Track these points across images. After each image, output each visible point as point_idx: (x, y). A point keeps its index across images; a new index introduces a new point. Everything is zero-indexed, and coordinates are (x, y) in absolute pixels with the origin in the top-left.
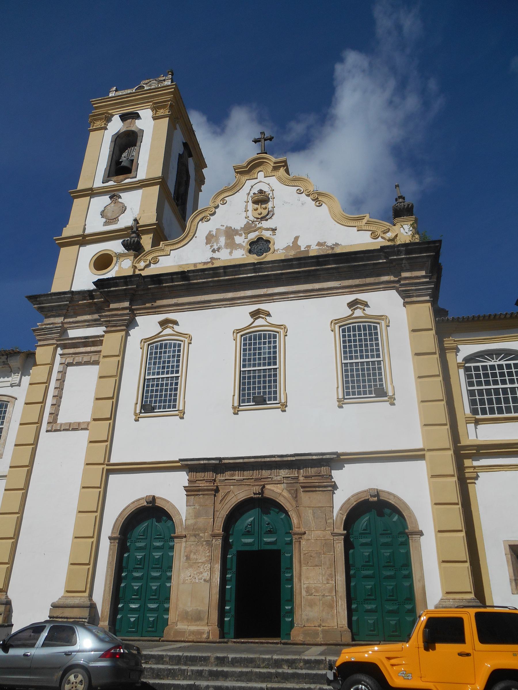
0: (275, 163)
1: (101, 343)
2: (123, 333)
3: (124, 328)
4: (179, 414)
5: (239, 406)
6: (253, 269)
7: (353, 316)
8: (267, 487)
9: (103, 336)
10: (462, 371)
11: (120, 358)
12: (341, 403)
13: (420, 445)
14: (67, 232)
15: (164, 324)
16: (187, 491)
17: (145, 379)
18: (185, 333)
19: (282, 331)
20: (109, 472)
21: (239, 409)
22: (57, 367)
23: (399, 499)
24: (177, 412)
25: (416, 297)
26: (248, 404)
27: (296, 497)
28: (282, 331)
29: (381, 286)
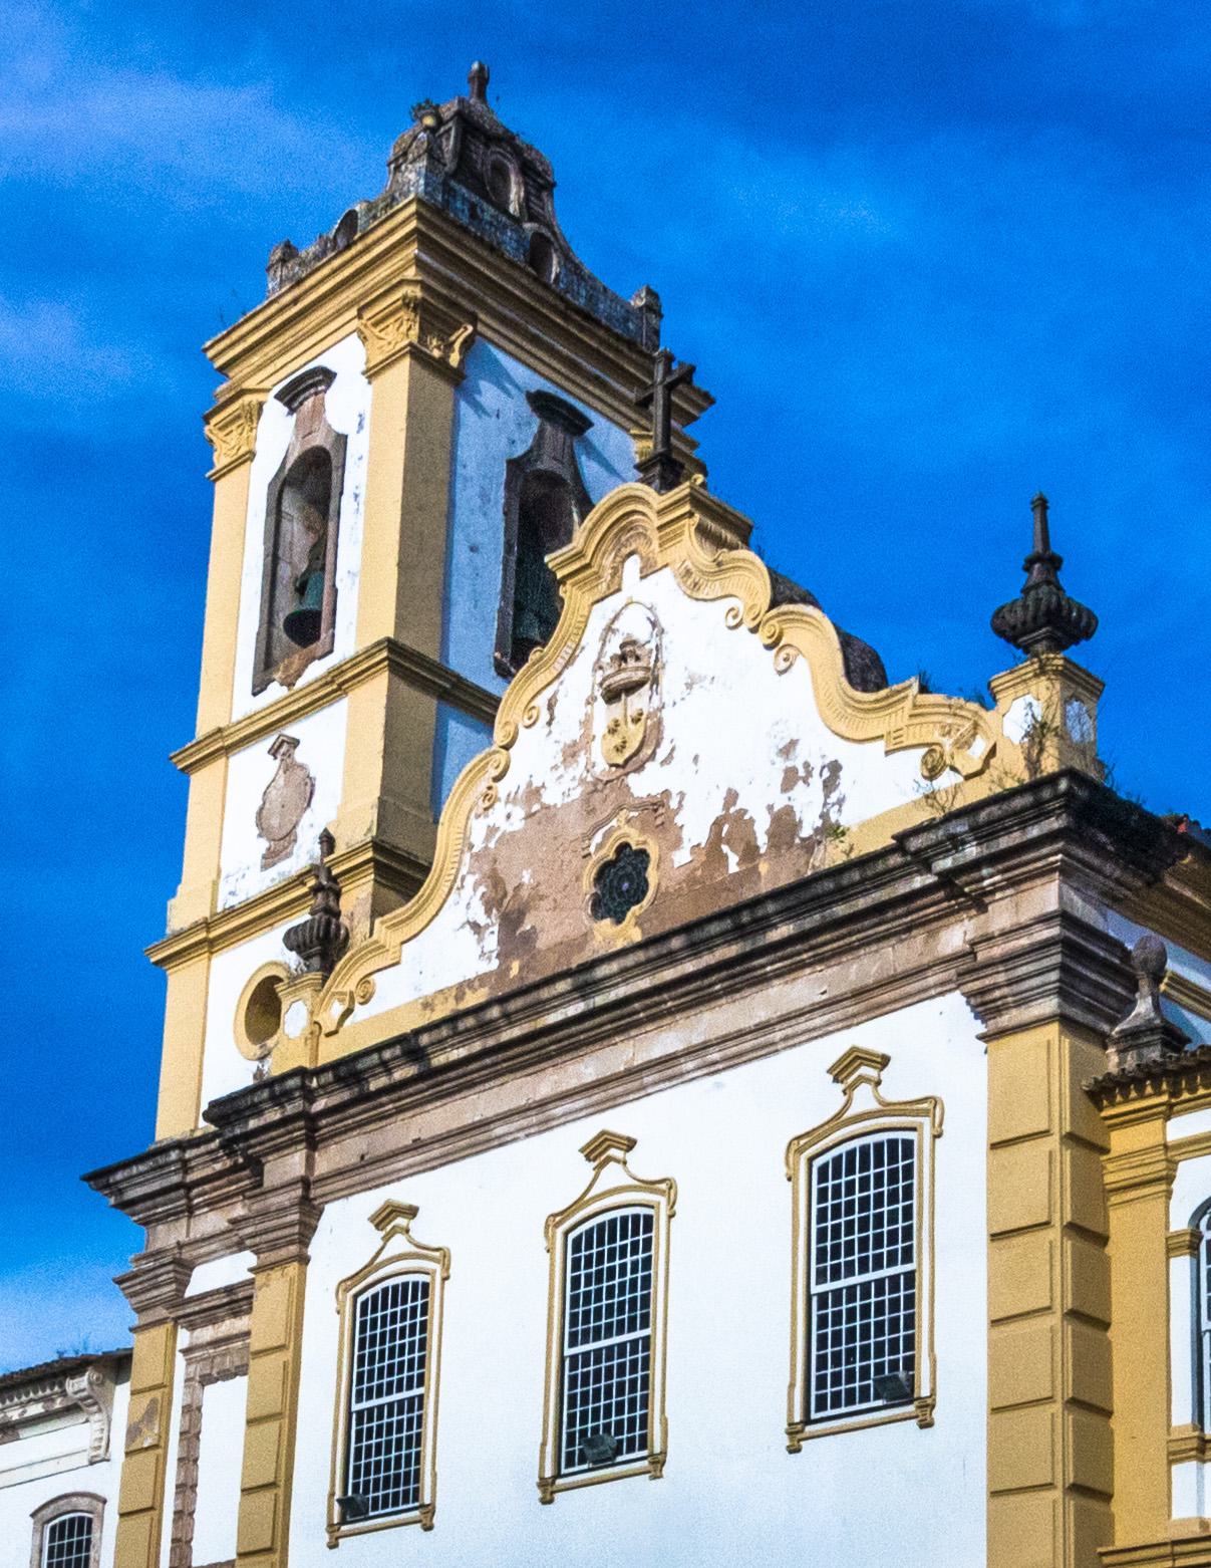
2: (293, 1269)
3: (293, 1249)
4: (919, 1412)
6: (575, 989)
7: (849, 1113)
9: (251, 1282)
11: (288, 1355)
14: (184, 910)
15: (387, 1218)
17: (349, 1414)
18: (436, 1246)
19: (663, 1200)
21: (554, 1488)
24: (645, 1463)
25: (1018, 1005)
26: (405, 1507)
28: (663, 1200)
29: (931, 981)
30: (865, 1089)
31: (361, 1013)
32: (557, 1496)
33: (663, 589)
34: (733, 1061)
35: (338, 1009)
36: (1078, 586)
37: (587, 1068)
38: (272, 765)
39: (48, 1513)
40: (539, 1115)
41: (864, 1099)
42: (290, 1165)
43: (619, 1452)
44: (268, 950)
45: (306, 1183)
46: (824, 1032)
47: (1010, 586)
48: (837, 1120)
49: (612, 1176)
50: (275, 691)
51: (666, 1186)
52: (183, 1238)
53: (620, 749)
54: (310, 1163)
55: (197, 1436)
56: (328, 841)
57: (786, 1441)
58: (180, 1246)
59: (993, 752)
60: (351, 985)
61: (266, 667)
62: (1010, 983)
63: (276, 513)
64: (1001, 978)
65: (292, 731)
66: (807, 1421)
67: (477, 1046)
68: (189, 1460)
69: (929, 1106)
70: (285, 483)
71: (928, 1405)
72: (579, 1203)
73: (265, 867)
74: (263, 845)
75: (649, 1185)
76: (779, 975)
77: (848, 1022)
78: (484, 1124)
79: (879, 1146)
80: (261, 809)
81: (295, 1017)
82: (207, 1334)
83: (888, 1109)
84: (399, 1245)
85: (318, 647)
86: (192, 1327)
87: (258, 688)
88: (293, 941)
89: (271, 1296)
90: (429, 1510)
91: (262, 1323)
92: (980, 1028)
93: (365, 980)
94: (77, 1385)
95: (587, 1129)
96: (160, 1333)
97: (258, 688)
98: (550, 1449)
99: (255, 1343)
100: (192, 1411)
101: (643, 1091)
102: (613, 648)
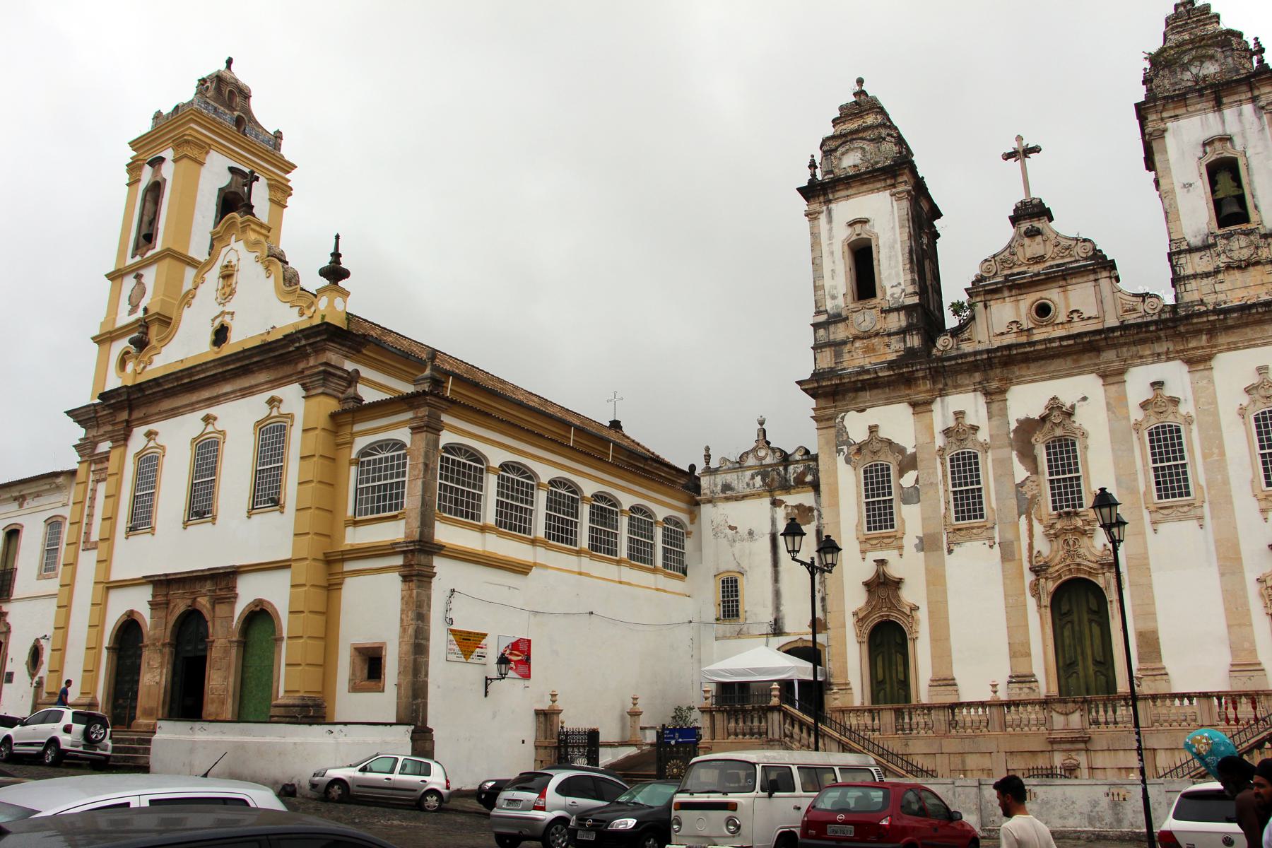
0: (241, 223)
1: (107, 459)
2: (122, 449)
3: (122, 442)
5: (189, 520)
8: (199, 599)
10: (353, 469)
12: (251, 512)
13: (288, 556)
16: (150, 605)
20: (108, 588)
22: (90, 485)
23: (275, 609)
27: (213, 608)
30: (275, 409)
31: (149, 368)
32: (188, 527)
33: (240, 246)
34: (243, 396)
35: (142, 365)
36: (345, 263)
37: (206, 394)
38: (134, 282)
39: (50, 521)
40: (192, 407)
41: (275, 413)
42: (124, 415)
43: (205, 514)
44: (123, 344)
45: (128, 422)
46: (267, 390)
47: (326, 261)
48: (268, 417)
49: (210, 428)
50: (138, 258)
51: (223, 433)
52: (95, 434)
53: (224, 294)
54: (130, 415)
55: (95, 499)
56: (146, 310)
57: (247, 514)
58: (94, 436)
59: (315, 312)
60: (146, 359)
61: (137, 249)
62: (311, 382)
63: (144, 200)
64: (308, 381)
65: (141, 272)
66: (253, 509)
67: (175, 384)
68: (92, 507)
69: (290, 416)
70: (147, 191)
71: (283, 507)
72: (201, 435)
73: (129, 315)
74: (130, 307)
75: (219, 432)
76: (257, 371)
77: (273, 388)
78: (178, 408)
79: (277, 426)
80: (130, 296)
81: (130, 367)
82: (100, 466)
83: (281, 416)
84: (152, 444)
85: (152, 245)
86: (96, 463)
87: (133, 257)
88: (131, 342)
89: (114, 456)
90: (153, 529)
91: (112, 466)
92: (304, 393)
93: (150, 358)
94: (60, 480)
95: (203, 413)
96: (86, 465)
97: (133, 257)
98: (187, 512)
99: (110, 471)
100: (94, 491)
101: (219, 403)
102: (225, 263)
